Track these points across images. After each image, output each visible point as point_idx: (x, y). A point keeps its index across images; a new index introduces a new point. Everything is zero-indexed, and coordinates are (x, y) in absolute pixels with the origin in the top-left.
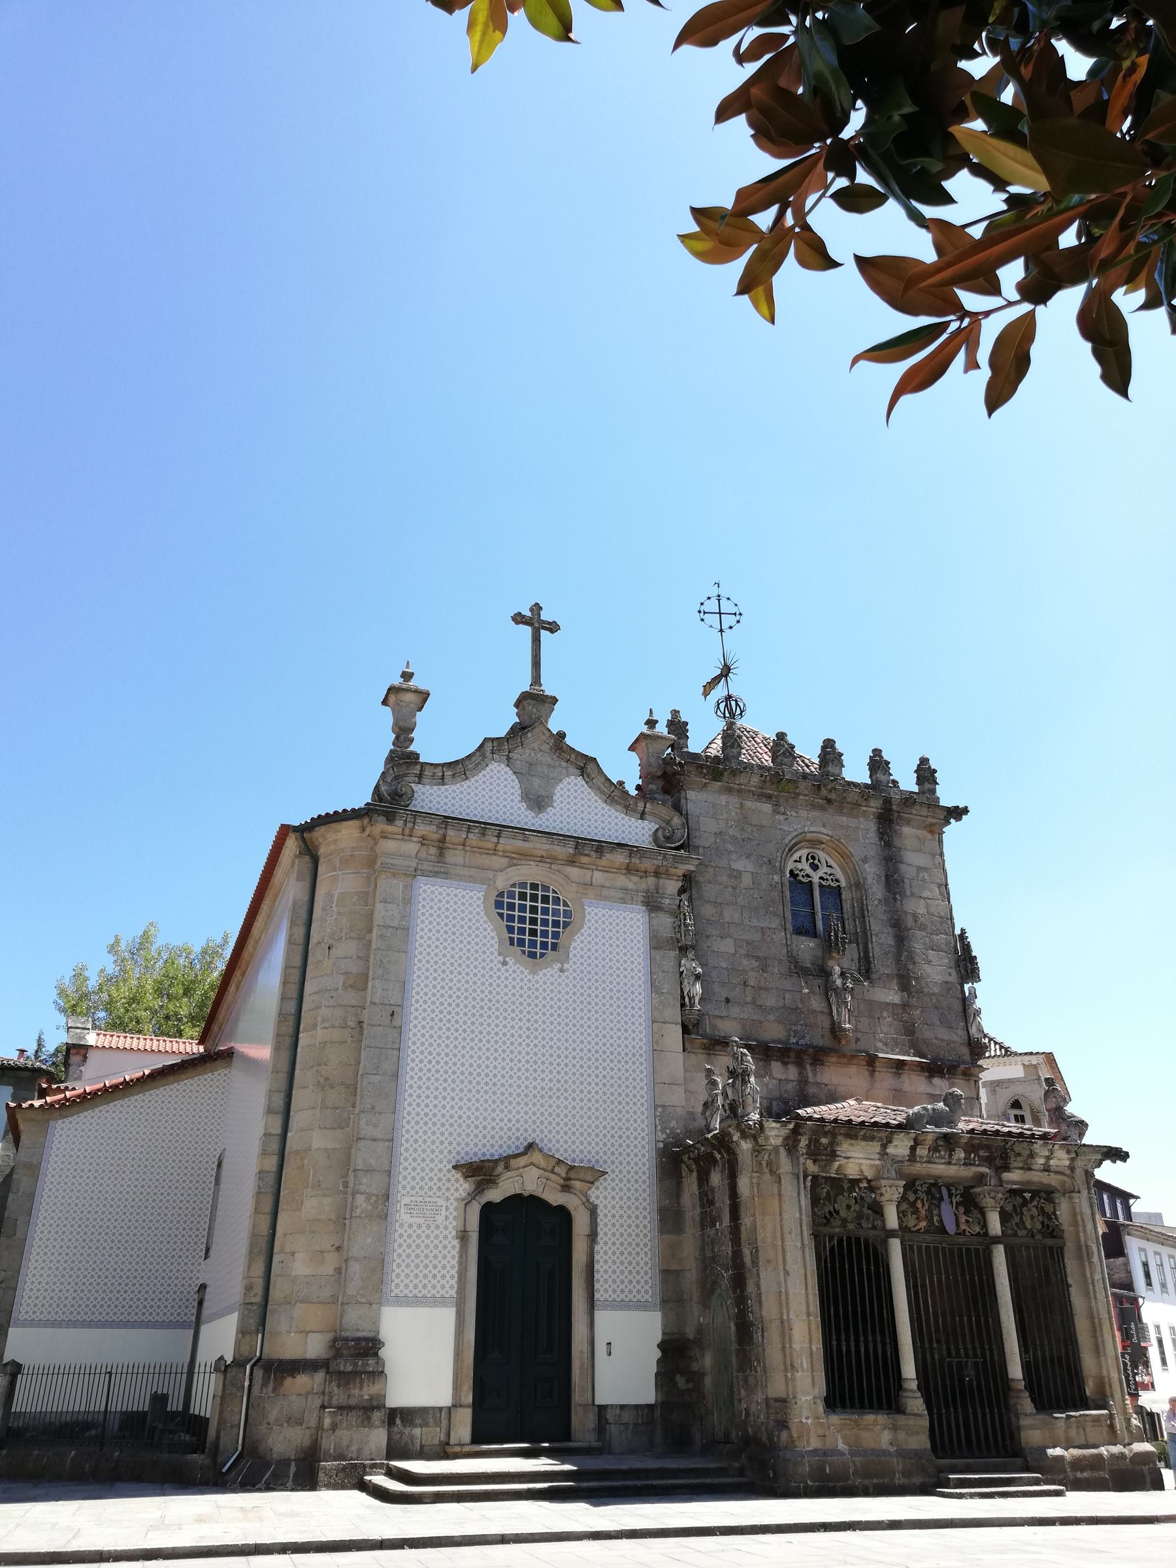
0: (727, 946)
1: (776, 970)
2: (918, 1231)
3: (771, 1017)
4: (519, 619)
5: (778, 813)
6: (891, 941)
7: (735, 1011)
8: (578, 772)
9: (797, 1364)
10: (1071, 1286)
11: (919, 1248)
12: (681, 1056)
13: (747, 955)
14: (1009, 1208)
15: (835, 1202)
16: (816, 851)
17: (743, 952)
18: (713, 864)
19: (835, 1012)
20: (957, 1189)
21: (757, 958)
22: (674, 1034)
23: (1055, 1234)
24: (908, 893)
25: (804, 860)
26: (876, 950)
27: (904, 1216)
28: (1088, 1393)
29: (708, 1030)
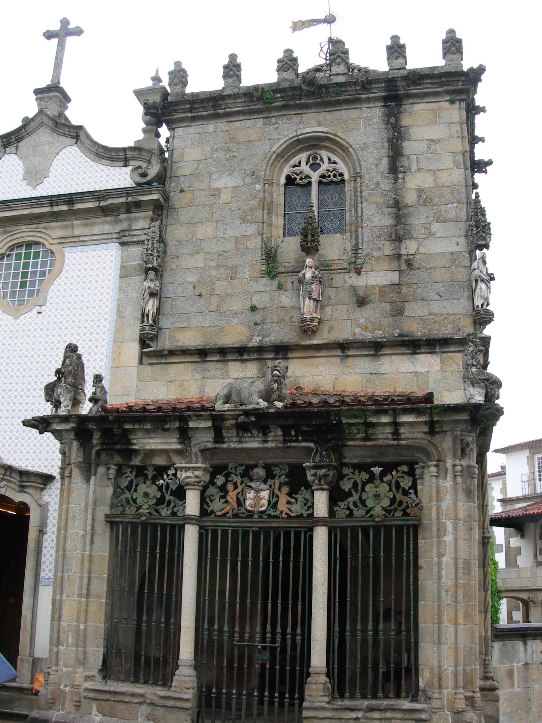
0: (198, 261)
1: (247, 275)
2: (224, 515)
3: (235, 321)
4: (49, 35)
5: (269, 125)
6: (389, 221)
7: (196, 322)
8: (75, 140)
9: (63, 636)
10: (422, 568)
11: (225, 533)
12: (135, 370)
13: (217, 267)
14: (346, 486)
15: (136, 490)
16: (318, 151)
17: (213, 264)
18: (191, 189)
19: (302, 304)
20: (281, 469)
21: (227, 268)
22: (134, 348)
23: (408, 511)
24: (414, 169)
25: (303, 163)
26: (366, 235)
27: (211, 501)
28: (421, 684)
29: (167, 343)
